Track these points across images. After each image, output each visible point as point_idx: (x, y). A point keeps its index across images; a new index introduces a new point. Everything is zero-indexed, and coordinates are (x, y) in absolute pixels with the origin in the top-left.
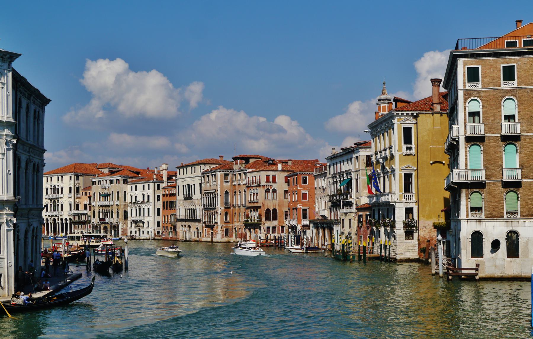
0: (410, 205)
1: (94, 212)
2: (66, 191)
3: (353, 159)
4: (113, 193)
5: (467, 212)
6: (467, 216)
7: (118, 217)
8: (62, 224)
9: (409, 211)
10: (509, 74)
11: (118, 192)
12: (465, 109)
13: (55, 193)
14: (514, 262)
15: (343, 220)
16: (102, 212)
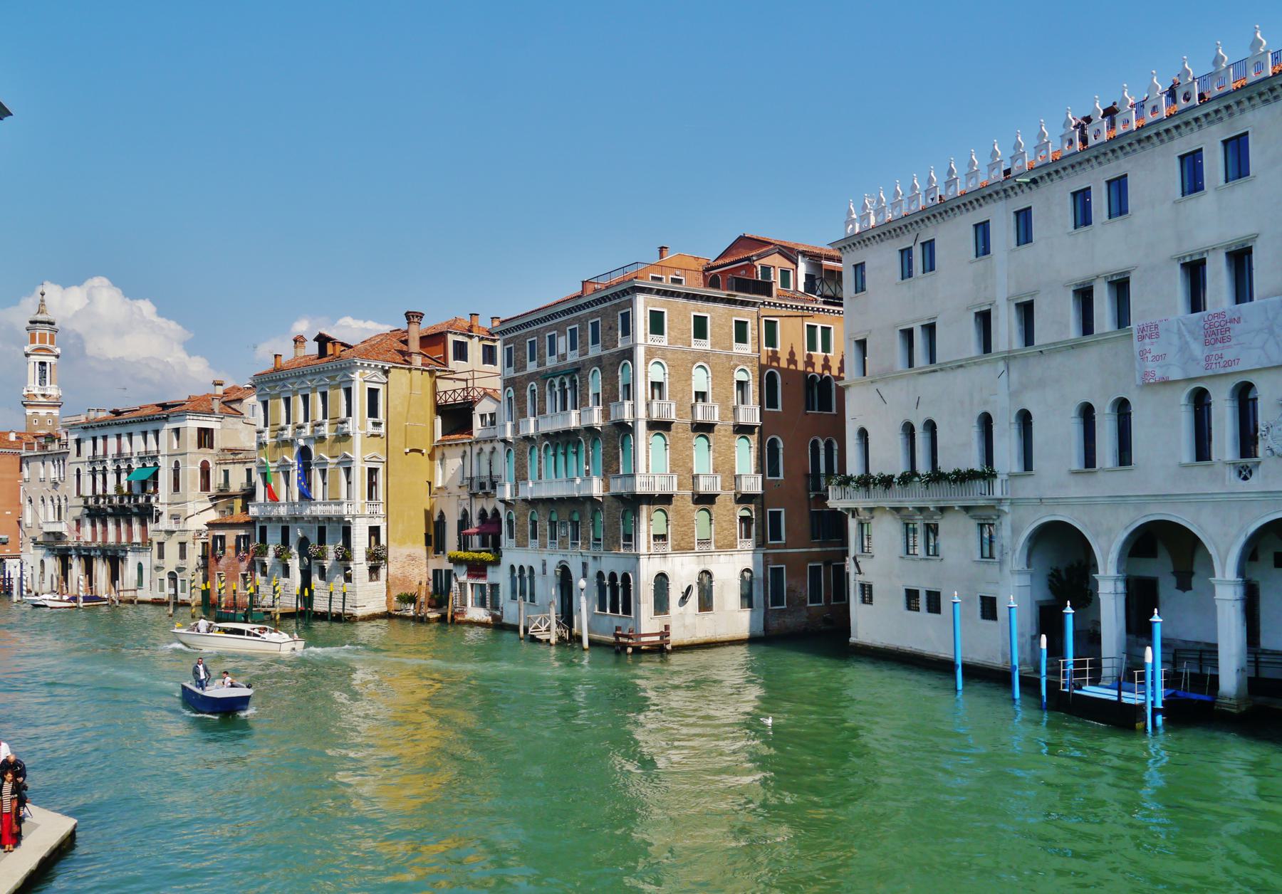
0: (376, 523)
3: (163, 435)
5: (649, 542)
6: (649, 548)
9: (374, 531)
10: (700, 328)
12: (646, 376)
14: (707, 616)
15: (161, 544)
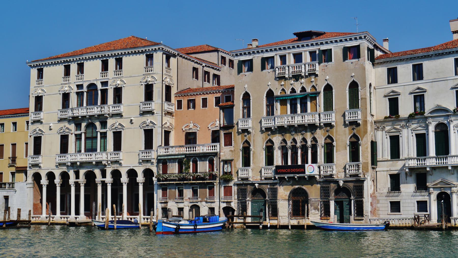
1: (246, 151)
2: (133, 96)
4: (328, 88)
7: (355, 156)
8: (117, 185)
11: (354, 86)
13: (92, 102)
16: (284, 149)
